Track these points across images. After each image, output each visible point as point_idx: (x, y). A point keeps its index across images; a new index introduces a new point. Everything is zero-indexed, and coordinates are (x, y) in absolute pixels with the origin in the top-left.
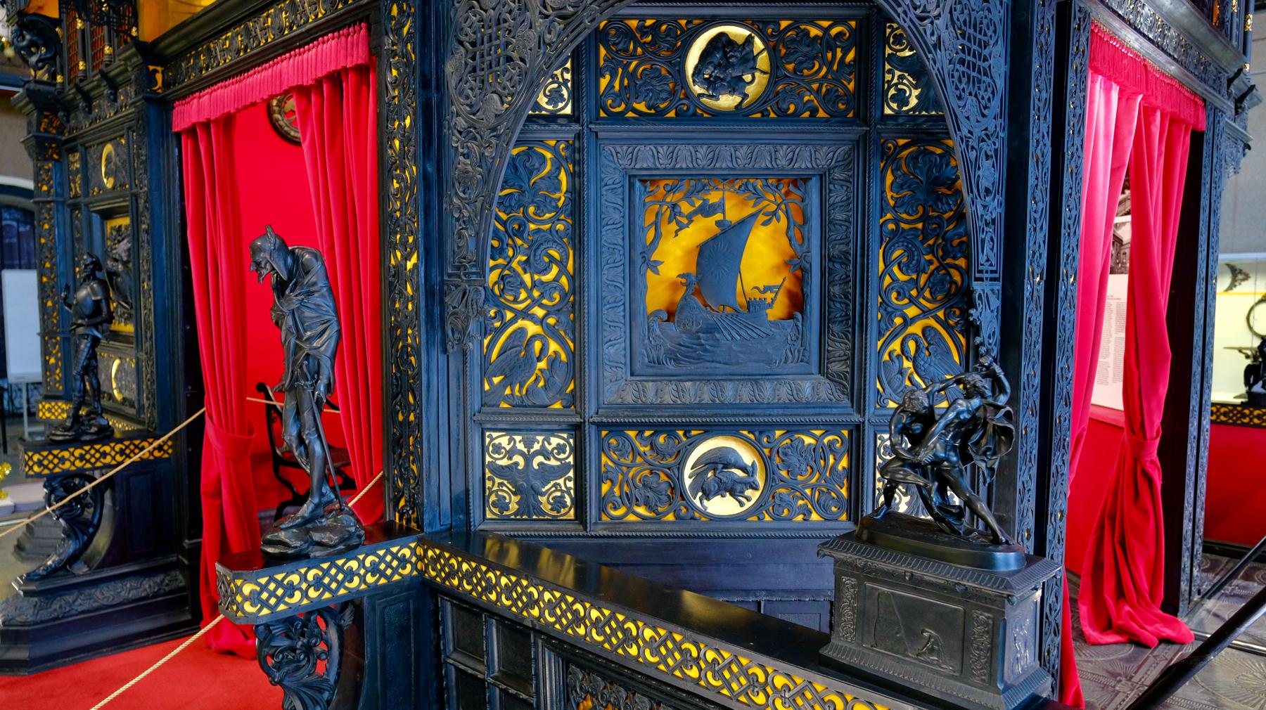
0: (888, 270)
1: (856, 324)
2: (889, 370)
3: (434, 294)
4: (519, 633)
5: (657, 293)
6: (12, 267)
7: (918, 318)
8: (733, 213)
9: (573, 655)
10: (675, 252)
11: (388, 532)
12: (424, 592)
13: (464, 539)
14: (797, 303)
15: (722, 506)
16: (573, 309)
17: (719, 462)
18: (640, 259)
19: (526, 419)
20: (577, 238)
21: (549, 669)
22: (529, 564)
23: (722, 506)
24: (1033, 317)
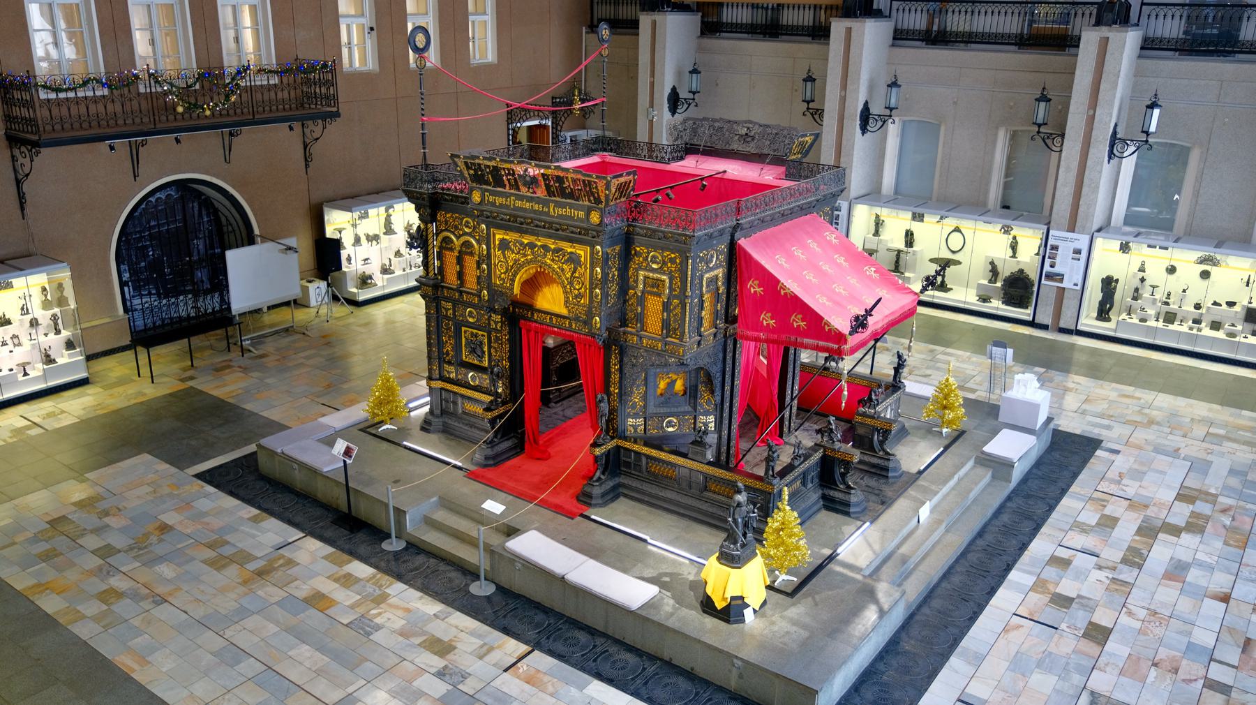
0: (701, 388)
1: (695, 398)
2: (702, 405)
3: (620, 395)
4: (636, 452)
5: (659, 391)
6: (230, 248)
7: (706, 395)
8: (674, 377)
9: (648, 457)
10: (662, 385)
11: (612, 438)
12: (618, 447)
13: (625, 438)
14: (685, 393)
15: (671, 429)
16: (644, 398)
17: (670, 422)
18: (657, 386)
19: (636, 416)
20: (646, 385)
21: (644, 459)
22: (635, 442)
23: (671, 429)
24: (727, 394)
